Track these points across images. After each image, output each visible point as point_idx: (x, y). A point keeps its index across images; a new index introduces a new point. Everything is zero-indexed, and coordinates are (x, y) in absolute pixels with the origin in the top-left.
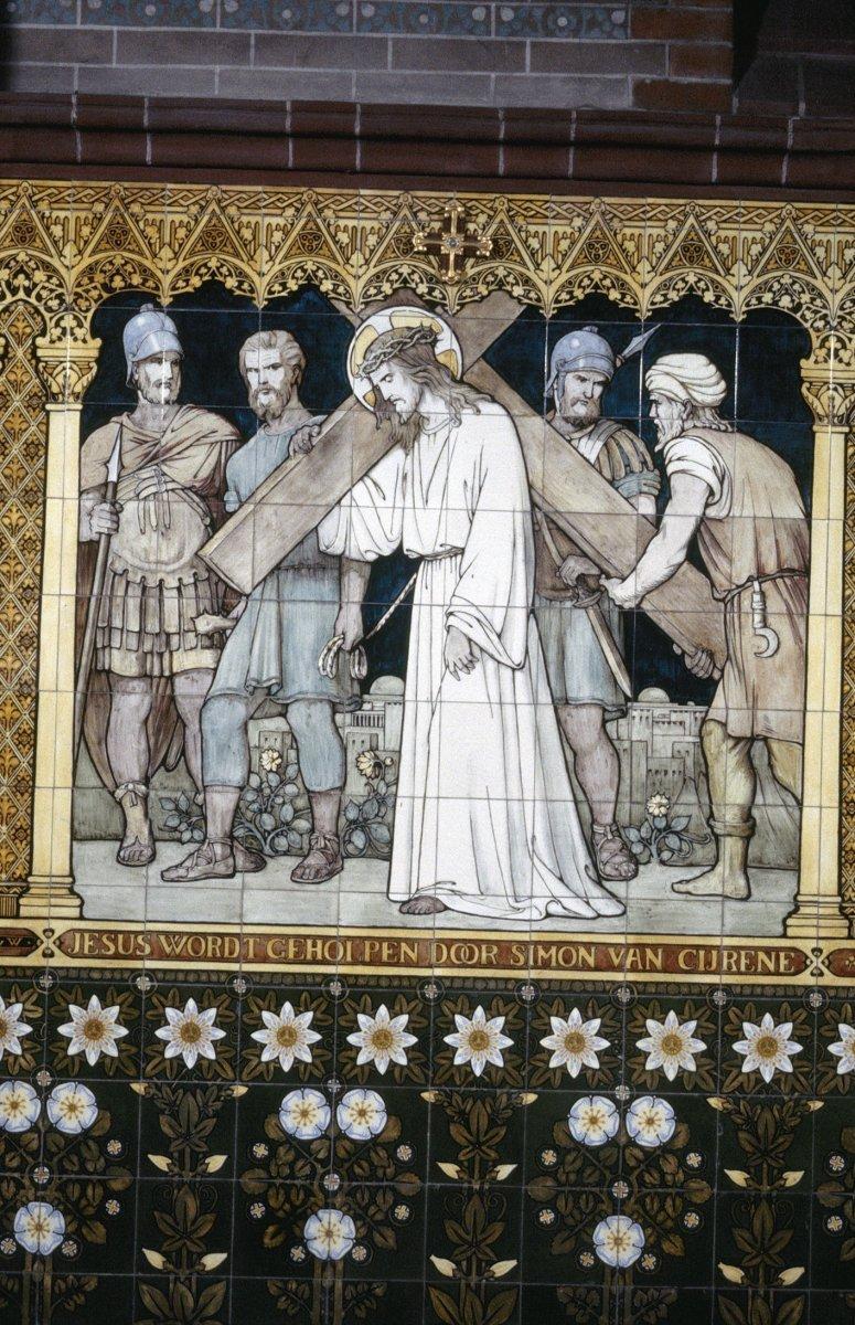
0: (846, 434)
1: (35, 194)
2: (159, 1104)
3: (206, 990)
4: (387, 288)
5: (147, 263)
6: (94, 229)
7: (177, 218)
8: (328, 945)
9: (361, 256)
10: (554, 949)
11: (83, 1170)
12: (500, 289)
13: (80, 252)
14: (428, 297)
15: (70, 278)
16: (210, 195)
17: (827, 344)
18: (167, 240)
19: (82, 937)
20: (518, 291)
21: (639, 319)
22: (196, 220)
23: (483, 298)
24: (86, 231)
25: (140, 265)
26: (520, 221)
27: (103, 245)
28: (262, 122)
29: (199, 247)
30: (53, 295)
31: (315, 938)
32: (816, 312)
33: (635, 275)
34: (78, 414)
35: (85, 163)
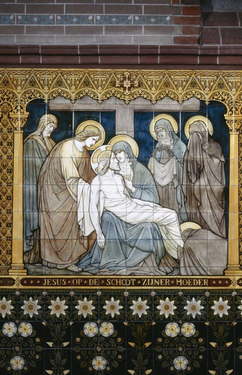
0: (239, 135)
1: (36, 73)
2: (132, 328)
3: (145, 295)
4: (108, 96)
5: (202, 92)
6: (187, 82)
7: (103, 79)
8: (122, 281)
9: (181, 88)
10: (181, 280)
11: (110, 347)
12: (194, 97)
13: (76, 88)
14: (201, 99)
15: (99, 95)
16: (138, 72)
17: (232, 110)
18: (154, 85)
19: (47, 281)
20: (199, 97)
21: (206, 104)
22: (162, 80)
23: (188, 99)
24: (184, 83)
25: (146, 92)
26: (226, 78)
27: (189, 87)
28: (153, 51)
29: (197, 87)
30: (230, 102)
31: (118, 279)
32: (229, 101)
33: (178, 91)
34: (238, 135)
35: (160, 64)
